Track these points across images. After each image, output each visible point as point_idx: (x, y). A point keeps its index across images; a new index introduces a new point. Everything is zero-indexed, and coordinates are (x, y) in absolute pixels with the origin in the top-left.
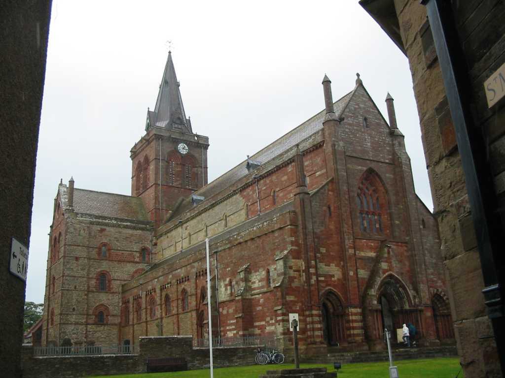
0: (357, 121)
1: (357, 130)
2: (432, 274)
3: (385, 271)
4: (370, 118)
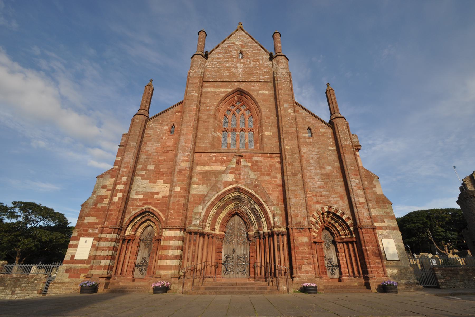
0: (230, 55)
1: (226, 61)
2: (320, 187)
3: (226, 184)
4: (246, 50)
